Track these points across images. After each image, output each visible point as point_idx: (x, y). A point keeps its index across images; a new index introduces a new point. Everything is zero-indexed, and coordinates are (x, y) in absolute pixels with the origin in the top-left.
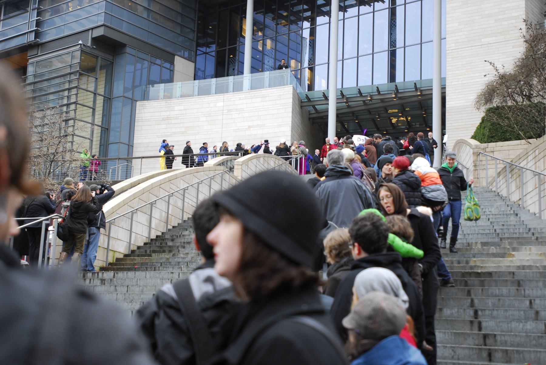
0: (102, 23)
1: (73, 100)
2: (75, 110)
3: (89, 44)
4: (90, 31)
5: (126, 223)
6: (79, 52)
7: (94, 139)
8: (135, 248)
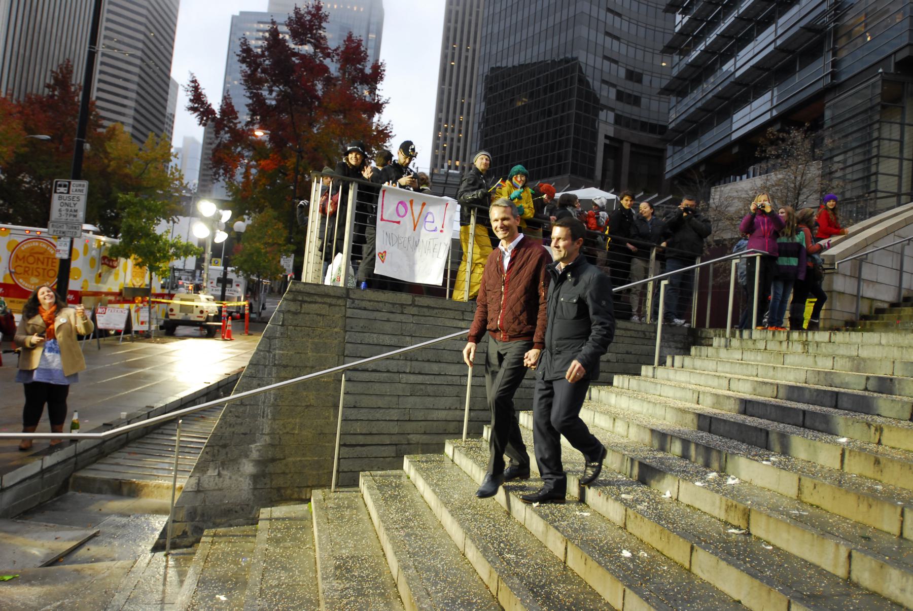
0: (906, 43)
1: (875, 135)
2: (878, 147)
3: (892, 70)
4: (893, 57)
5: (890, 261)
6: (880, 82)
7: (904, 176)
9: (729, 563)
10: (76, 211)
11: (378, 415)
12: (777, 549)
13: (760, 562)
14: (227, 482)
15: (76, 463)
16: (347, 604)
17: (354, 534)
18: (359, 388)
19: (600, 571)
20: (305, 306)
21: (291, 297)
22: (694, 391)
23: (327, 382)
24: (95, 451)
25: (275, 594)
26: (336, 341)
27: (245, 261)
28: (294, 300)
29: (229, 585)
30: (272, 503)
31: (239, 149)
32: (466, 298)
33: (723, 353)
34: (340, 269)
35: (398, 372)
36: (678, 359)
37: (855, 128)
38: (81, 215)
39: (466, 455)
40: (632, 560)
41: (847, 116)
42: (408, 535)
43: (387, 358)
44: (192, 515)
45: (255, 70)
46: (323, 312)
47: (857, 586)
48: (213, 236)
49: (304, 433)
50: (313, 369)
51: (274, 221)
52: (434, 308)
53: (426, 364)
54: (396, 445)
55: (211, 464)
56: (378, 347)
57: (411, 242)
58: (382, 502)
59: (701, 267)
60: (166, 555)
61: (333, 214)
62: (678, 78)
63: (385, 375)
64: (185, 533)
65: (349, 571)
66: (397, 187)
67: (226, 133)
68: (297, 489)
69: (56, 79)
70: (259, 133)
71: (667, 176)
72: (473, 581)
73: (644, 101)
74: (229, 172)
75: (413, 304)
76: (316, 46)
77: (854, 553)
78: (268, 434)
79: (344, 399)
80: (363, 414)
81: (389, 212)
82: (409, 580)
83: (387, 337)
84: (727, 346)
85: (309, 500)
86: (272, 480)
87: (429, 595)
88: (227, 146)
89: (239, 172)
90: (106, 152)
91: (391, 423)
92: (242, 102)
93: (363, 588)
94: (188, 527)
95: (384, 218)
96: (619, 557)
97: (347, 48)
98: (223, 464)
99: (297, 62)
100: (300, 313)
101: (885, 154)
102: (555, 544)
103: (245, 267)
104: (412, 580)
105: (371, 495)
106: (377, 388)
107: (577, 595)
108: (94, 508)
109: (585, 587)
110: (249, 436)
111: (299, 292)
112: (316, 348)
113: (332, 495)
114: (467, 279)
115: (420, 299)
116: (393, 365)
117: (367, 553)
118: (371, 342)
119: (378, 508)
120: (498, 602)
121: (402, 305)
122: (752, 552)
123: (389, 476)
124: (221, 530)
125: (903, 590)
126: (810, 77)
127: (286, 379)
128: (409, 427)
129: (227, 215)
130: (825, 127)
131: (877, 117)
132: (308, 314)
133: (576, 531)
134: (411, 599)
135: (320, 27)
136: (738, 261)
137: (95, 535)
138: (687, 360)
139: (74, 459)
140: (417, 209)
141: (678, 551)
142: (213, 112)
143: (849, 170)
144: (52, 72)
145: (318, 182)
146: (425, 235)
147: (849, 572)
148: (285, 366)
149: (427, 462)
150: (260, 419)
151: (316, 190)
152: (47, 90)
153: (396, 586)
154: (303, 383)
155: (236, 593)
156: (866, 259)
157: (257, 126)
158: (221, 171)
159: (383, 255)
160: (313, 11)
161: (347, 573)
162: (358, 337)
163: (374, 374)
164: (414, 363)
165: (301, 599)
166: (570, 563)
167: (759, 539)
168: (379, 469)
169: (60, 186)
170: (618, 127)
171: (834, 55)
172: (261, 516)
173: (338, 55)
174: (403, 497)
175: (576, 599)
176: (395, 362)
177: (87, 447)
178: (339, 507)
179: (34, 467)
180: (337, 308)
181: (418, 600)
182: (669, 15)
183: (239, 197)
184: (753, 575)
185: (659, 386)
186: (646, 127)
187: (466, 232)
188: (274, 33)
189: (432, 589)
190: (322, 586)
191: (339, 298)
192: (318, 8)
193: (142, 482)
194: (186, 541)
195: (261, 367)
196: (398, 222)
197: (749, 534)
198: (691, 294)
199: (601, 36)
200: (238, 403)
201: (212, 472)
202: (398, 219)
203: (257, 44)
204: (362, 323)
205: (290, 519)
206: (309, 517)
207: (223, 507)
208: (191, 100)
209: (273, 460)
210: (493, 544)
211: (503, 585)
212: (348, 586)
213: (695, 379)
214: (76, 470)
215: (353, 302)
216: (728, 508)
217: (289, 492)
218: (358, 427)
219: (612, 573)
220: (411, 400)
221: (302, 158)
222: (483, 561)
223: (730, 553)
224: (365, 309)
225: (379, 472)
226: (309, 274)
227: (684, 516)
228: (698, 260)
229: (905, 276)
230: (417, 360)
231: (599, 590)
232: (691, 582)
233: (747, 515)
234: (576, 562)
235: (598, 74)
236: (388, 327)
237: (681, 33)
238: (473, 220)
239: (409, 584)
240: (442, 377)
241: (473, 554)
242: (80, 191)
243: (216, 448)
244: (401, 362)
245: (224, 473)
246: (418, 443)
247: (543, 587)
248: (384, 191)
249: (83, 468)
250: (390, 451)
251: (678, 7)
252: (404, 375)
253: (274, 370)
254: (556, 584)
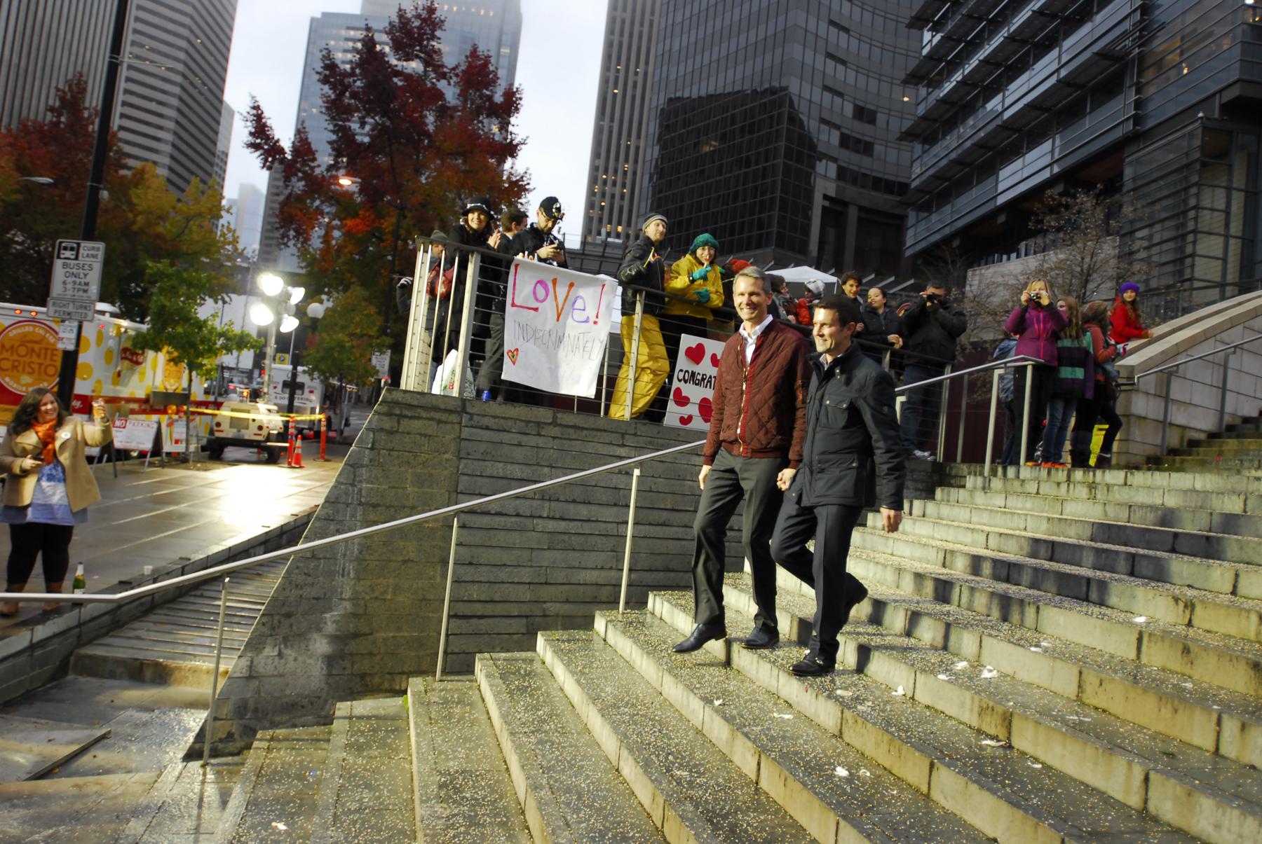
1: (1192, 202)
2: (1196, 218)
3: (1217, 115)
4: (1218, 96)
5: (1210, 375)
6: (1200, 131)
8: (1238, 422)
9: (982, 786)
10: (87, 284)
11: (503, 575)
12: (1047, 767)
13: (1024, 785)
14: (291, 665)
15: (79, 636)
16: (454, 837)
17: (466, 740)
18: (477, 537)
19: (806, 795)
20: (404, 422)
21: (385, 409)
22: (938, 549)
23: (432, 529)
25: (355, 822)
26: (446, 472)
27: (323, 358)
28: (389, 414)
29: (291, 808)
30: (352, 695)
31: (317, 203)
32: (627, 416)
33: (980, 498)
34: (453, 372)
35: (532, 517)
36: (917, 504)
37: (1165, 193)
38: (94, 289)
39: (624, 633)
40: (849, 780)
41: (1155, 176)
42: (541, 742)
43: (517, 497)
44: (241, 710)
45: (342, 94)
46: (429, 431)
47: (1155, 820)
48: (279, 322)
49: (400, 598)
50: (413, 510)
51: (363, 304)
52: (583, 429)
53: (571, 506)
54: (527, 617)
55: (270, 640)
56: (505, 482)
57: (553, 337)
58: (505, 696)
59: (952, 379)
60: (203, 766)
61: (446, 297)
62: (925, 118)
63: (514, 519)
64: (230, 736)
65: (457, 790)
66: (536, 261)
67: (300, 180)
68: (388, 677)
69: (63, 99)
70: (345, 182)
71: (908, 253)
72: (630, 806)
73: (878, 149)
74: (303, 235)
75: (554, 423)
76: (427, 63)
77: (1152, 775)
78: (349, 600)
79: (456, 553)
80: (483, 574)
81: (523, 294)
82: (541, 805)
83: (517, 468)
84: (984, 489)
85: (405, 692)
86: (353, 663)
87: (568, 825)
88: (300, 199)
89: (317, 234)
90: (131, 204)
91: (521, 586)
92: (322, 138)
93: (476, 815)
94: (234, 727)
95: (516, 302)
96: (832, 776)
97: (470, 66)
98: (285, 640)
99: (400, 84)
100: (397, 431)
101: (1205, 229)
102: (744, 758)
103: (323, 367)
104: (546, 804)
105: (491, 686)
106: (502, 538)
107: (773, 828)
108: (104, 698)
109: (784, 817)
110: (323, 602)
111: (397, 403)
112: (419, 482)
113: (437, 685)
114: (630, 389)
115: (565, 416)
116: (524, 506)
117: (484, 766)
118: (495, 474)
119: (500, 704)
120: (664, 836)
121: (539, 424)
122: (1013, 771)
123: (517, 660)
124: (281, 732)
125: (1218, 827)
126: (1105, 121)
127: (376, 523)
128: (546, 593)
129: (298, 294)
130: (1125, 189)
131: (1195, 179)
132: (408, 433)
133: (772, 739)
134: (543, 831)
135: (433, 37)
136: (1001, 371)
137: (104, 737)
138: (931, 507)
139: (77, 630)
140: (562, 291)
141: (912, 769)
142: (282, 151)
143: (1155, 250)
144: (58, 89)
145: (426, 251)
146: (572, 328)
147: (1146, 801)
148: (375, 506)
149: (569, 641)
150: (339, 579)
151: (423, 262)
152: (49, 115)
153: (523, 813)
154: (400, 529)
155: (300, 821)
156: (1177, 371)
157: (342, 172)
158: (292, 233)
159: (514, 353)
160: (424, 14)
161: (455, 793)
162: (476, 467)
163: (498, 519)
164: (554, 504)
165: (391, 829)
166: (764, 784)
167: (1023, 753)
168: (504, 650)
169: (65, 249)
170: (842, 184)
171: (1138, 92)
172: (338, 713)
173: (457, 75)
174: (535, 689)
175: (772, 833)
176: (528, 502)
177: (96, 614)
178: (446, 701)
179: (21, 639)
180: (449, 426)
181: (554, 832)
182: (914, 31)
183: (316, 269)
184: (1015, 804)
185: (891, 542)
186: (879, 184)
187: (630, 325)
188: (369, 43)
189: (572, 818)
190: (420, 811)
191: (451, 412)
192: (431, 10)
193: (172, 663)
194: (232, 747)
195: (341, 506)
196: (536, 309)
197: (1010, 747)
198: (937, 416)
199: (820, 58)
200: (309, 555)
201: (270, 651)
202: (535, 305)
203: (345, 58)
204: (483, 447)
205: (377, 717)
206: (404, 715)
207: (284, 700)
208: (251, 134)
209: (356, 635)
210: (658, 756)
211: (670, 813)
212: (456, 811)
213: (940, 533)
214: (79, 645)
215: (471, 419)
216: (982, 711)
217: (377, 680)
218: (475, 592)
219: (822, 797)
220: (548, 554)
221: (405, 217)
222: (644, 779)
223: (983, 773)
224: (487, 428)
225: (503, 655)
226: (410, 379)
227: (921, 722)
228: (948, 368)
229: (1229, 396)
230: (558, 500)
231: (803, 821)
232: (929, 812)
233: (1008, 720)
234: (773, 783)
235: (815, 111)
236: (519, 453)
237: (930, 56)
238: (639, 308)
239: (540, 810)
240: (593, 524)
241: (629, 769)
242: (93, 256)
243: (277, 618)
244: (536, 503)
245: (287, 652)
246: (557, 615)
247: (725, 817)
248: (517, 266)
249: (90, 642)
250: (518, 625)
251: (927, 22)
252: (540, 521)
253: (360, 511)
254: (745, 813)
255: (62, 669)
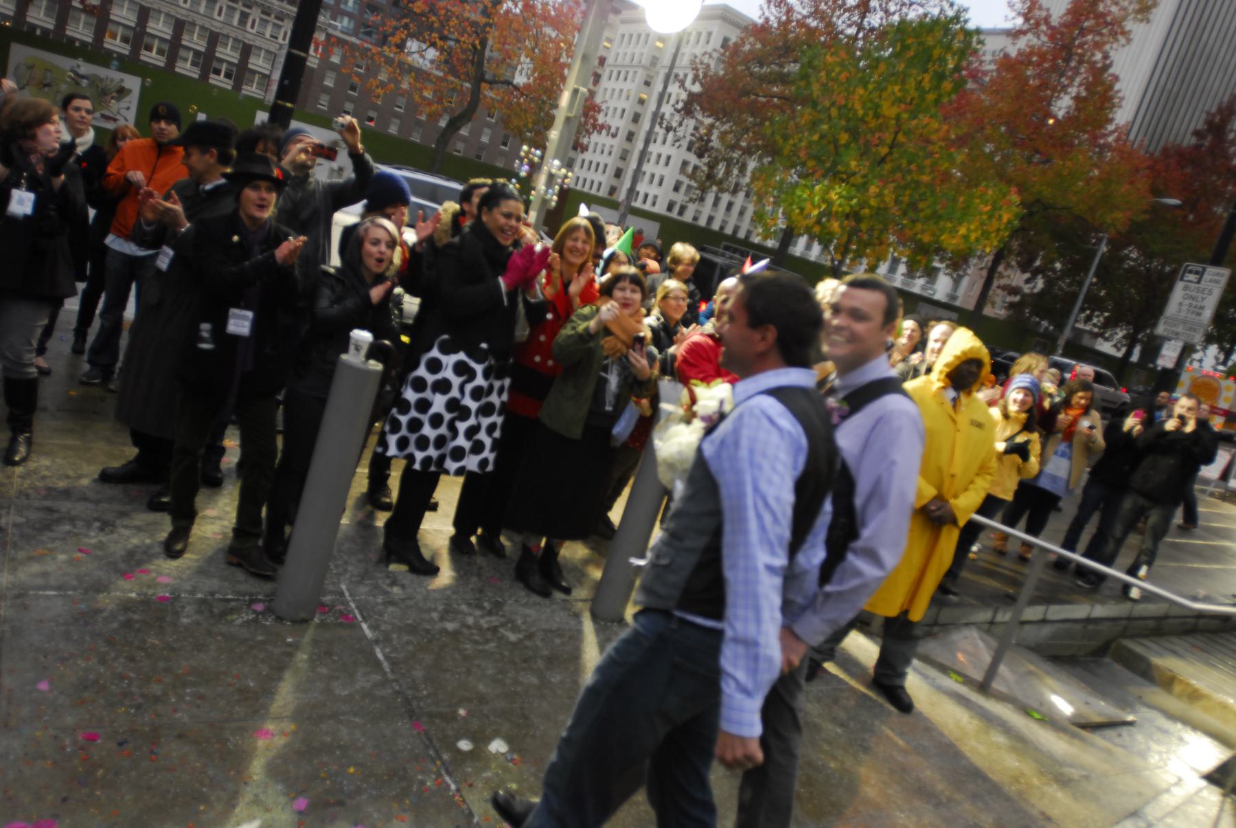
15: (1125, 628)
24: (1151, 623)
108: (1134, 690)
137: (1131, 724)
139: (1124, 622)
144: (1208, 113)
169: (1190, 272)
179: (1079, 610)
242: (1217, 282)
249: (1132, 637)
255: (1102, 651)
